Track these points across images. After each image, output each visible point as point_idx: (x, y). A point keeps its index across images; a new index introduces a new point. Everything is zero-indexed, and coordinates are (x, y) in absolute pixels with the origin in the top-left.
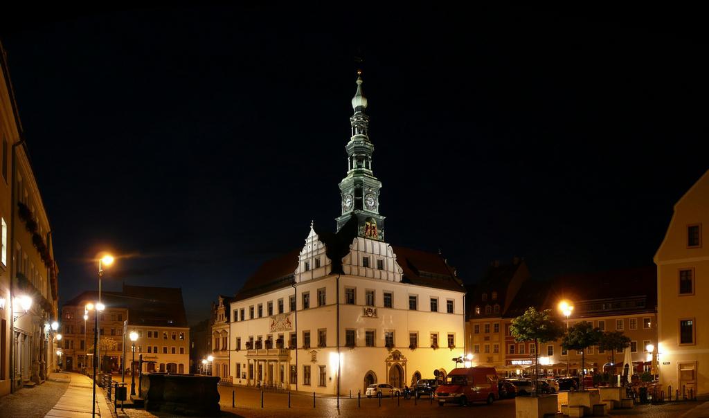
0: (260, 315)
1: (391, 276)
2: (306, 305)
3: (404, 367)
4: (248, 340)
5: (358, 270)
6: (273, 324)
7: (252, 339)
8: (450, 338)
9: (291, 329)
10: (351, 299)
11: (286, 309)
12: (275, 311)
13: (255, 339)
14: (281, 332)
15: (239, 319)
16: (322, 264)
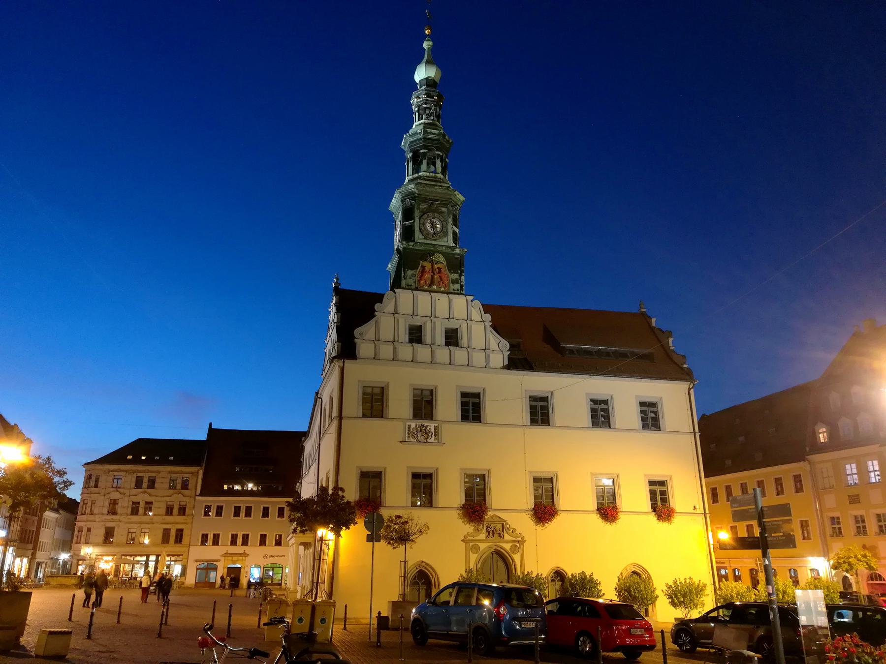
1: (479, 358)
3: (516, 557)
5: (395, 351)
8: (658, 489)
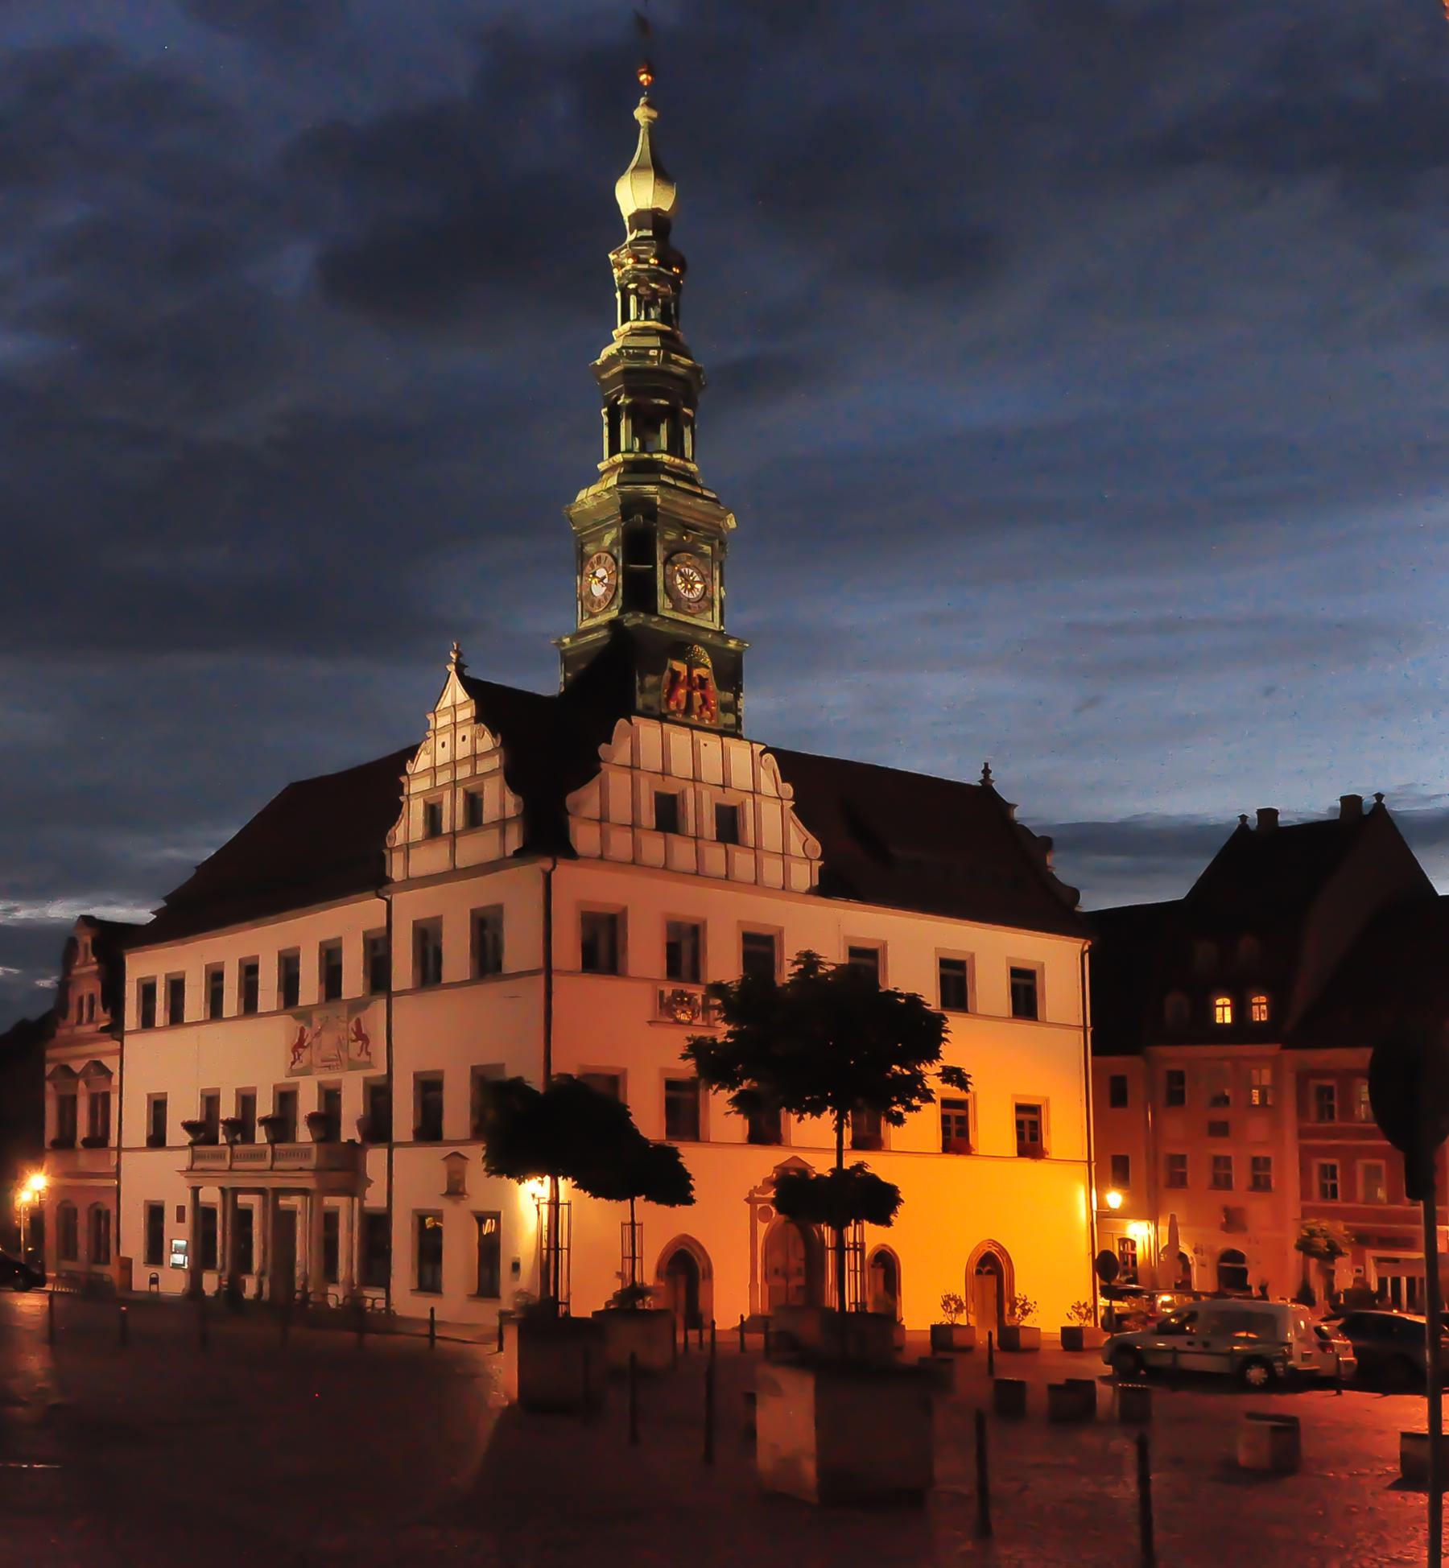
0: (249, 1003)
1: (772, 871)
2: (429, 971)
4: (195, 1115)
5: (636, 846)
6: (299, 1045)
7: (211, 1101)
8: (1028, 1117)
9: (369, 1065)
10: (603, 945)
11: (353, 982)
12: (310, 990)
13: (228, 1110)
14: (330, 1077)
15: (161, 1016)
16: (490, 812)
